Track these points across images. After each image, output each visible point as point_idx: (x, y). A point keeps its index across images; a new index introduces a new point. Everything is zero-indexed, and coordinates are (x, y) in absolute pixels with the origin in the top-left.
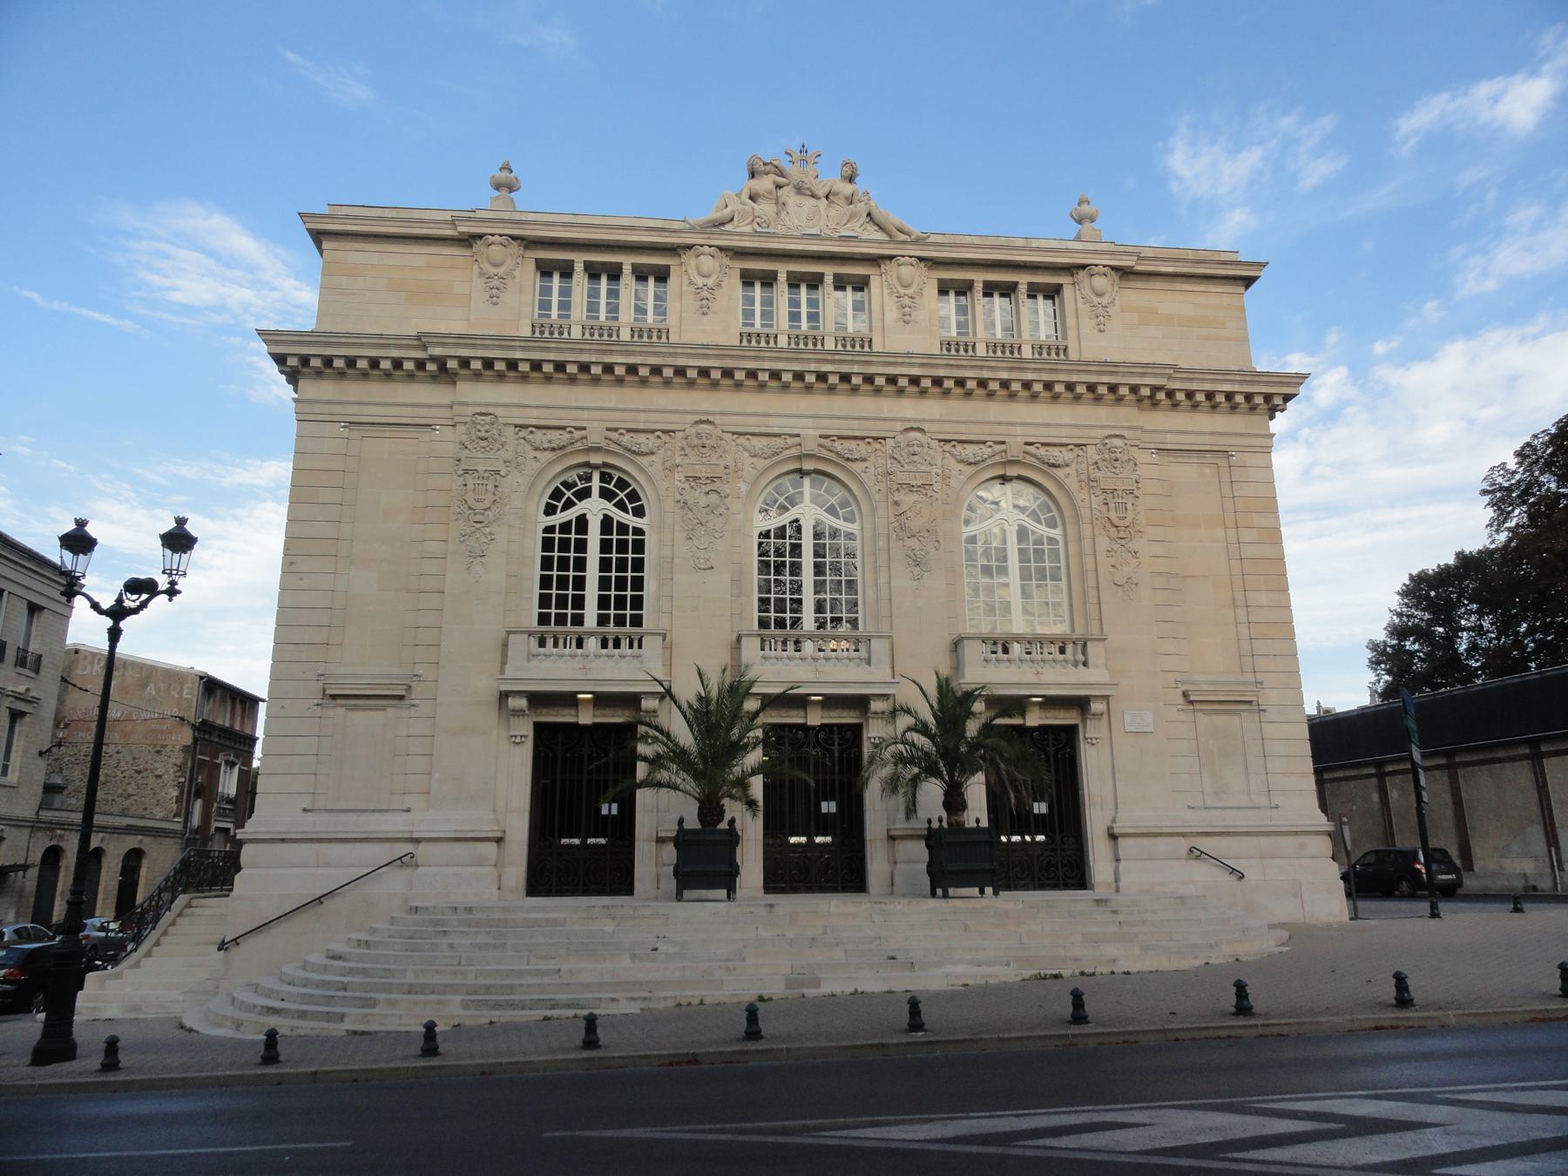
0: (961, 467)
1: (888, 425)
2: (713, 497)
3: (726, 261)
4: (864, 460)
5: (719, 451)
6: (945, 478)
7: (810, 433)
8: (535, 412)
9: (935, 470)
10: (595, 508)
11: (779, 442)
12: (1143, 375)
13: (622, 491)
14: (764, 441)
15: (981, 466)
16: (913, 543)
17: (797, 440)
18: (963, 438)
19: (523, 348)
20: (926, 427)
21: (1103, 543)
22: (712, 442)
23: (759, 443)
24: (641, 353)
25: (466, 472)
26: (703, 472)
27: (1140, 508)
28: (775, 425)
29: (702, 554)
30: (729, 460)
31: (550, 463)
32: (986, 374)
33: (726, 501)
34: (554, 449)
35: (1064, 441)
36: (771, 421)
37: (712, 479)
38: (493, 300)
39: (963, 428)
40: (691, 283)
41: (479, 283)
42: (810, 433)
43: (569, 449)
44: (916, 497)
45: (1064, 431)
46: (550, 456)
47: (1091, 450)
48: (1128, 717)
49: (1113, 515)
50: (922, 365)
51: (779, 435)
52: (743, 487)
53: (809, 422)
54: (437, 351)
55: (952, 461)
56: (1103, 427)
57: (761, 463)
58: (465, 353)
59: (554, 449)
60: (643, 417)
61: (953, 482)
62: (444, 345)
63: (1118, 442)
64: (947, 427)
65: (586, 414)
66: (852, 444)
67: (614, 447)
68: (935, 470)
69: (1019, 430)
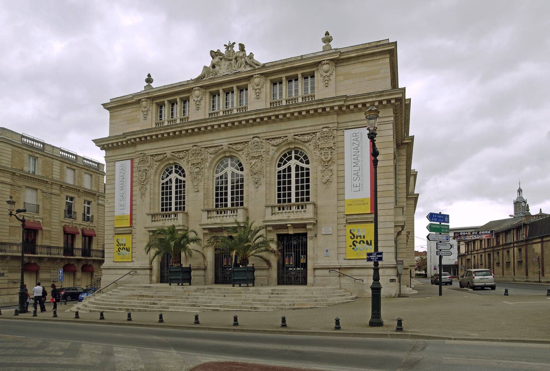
0: (273, 147)
1: (249, 137)
2: (198, 170)
3: (203, 90)
4: (242, 150)
5: (200, 154)
6: (267, 152)
7: (225, 143)
8: (154, 151)
9: (263, 150)
10: (174, 176)
11: (217, 149)
12: (334, 102)
13: (180, 171)
14: (214, 149)
15: (280, 146)
16: (256, 176)
17: (221, 147)
18: (273, 137)
19: (147, 132)
20: (260, 136)
21: (320, 168)
22: (198, 152)
23: (211, 150)
24: (175, 128)
25: (139, 171)
26: (195, 162)
27: (335, 152)
28: (216, 143)
29: (196, 187)
30: (203, 157)
31: (160, 165)
32: (277, 113)
33: (203, 170)
34: (159, 161)
35: (308, 132)
36: (214, 142)
37: (198, 163)
38: (145, 118)
39: (273, 133)
40: (194, 100)
41: (142, 114)
42: (225, 143)
43: (164, 160)
44: (257, 160)
45: (308, 129)
46: (159, 163)
47: (318, 134)
48: (323, 229)
49: (323, 158)
50: (255, 114)
51: (217, 146)
52: (208, 164)
53: (225, 140)
54: (128, 138)
55: (270, 146)
56: (322, 124)
57: (213, 156)
58: (134, 137)
59: (159, 161)
60: (180, 147)
61: (271, 153)
62: (129, 136)
63: (325, 130)
64: (268, 134)
65: (166, 149)
66: (238, 146)
67: (174, 158)
68: (263, 150)
69: (292, 131)
